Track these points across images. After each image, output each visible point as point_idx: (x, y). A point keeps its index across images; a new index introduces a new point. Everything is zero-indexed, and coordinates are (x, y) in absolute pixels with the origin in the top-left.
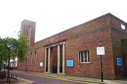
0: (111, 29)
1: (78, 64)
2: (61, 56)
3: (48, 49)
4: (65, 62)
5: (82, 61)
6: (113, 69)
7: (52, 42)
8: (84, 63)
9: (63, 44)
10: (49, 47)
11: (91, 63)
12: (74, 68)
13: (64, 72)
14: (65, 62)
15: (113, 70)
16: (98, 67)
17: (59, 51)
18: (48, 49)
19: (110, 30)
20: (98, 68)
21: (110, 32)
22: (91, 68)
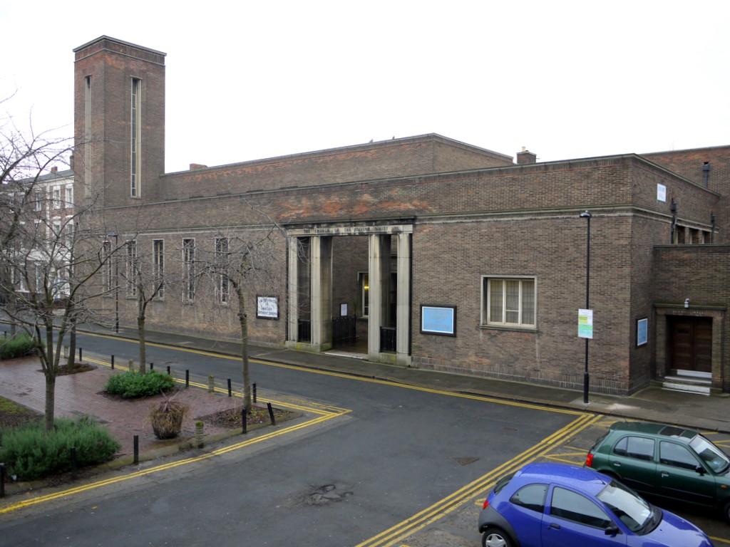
0: (634, 216)
1: (478, 328)
2: (390, 280)
3: (305, 241)
4: (414, 317)
5: (496, 316)
6: (624, 359)
7: (334, 215)
8: (503, 323)
9: (397, 233)
10: (312, 232)
11: (538, 332)
12: (459, 342)
13: (406, 350)
14: (414, 317)
15: (625, 364)
16: (566, 347)
17: (377, 261)
18: (305, 241)
19: (630, 220)
20: (566, 350)
21: (626, 228)
22: (537, 346)
